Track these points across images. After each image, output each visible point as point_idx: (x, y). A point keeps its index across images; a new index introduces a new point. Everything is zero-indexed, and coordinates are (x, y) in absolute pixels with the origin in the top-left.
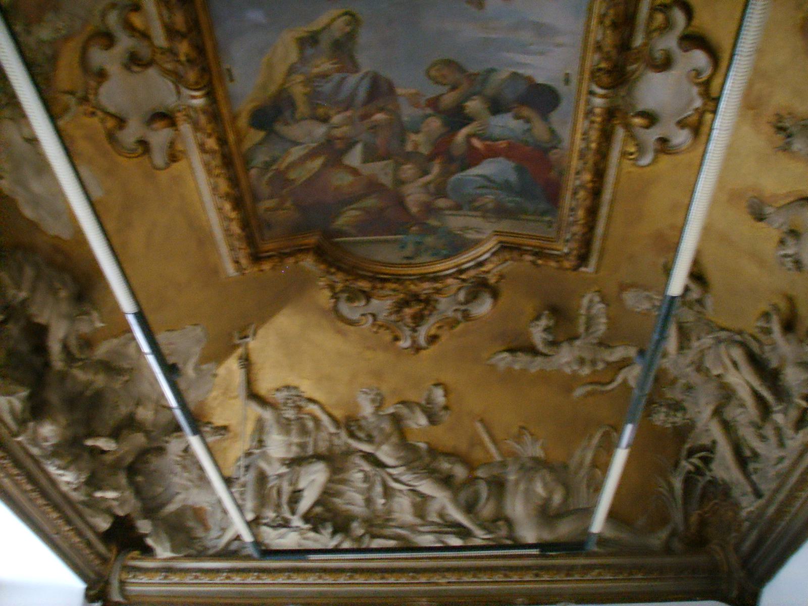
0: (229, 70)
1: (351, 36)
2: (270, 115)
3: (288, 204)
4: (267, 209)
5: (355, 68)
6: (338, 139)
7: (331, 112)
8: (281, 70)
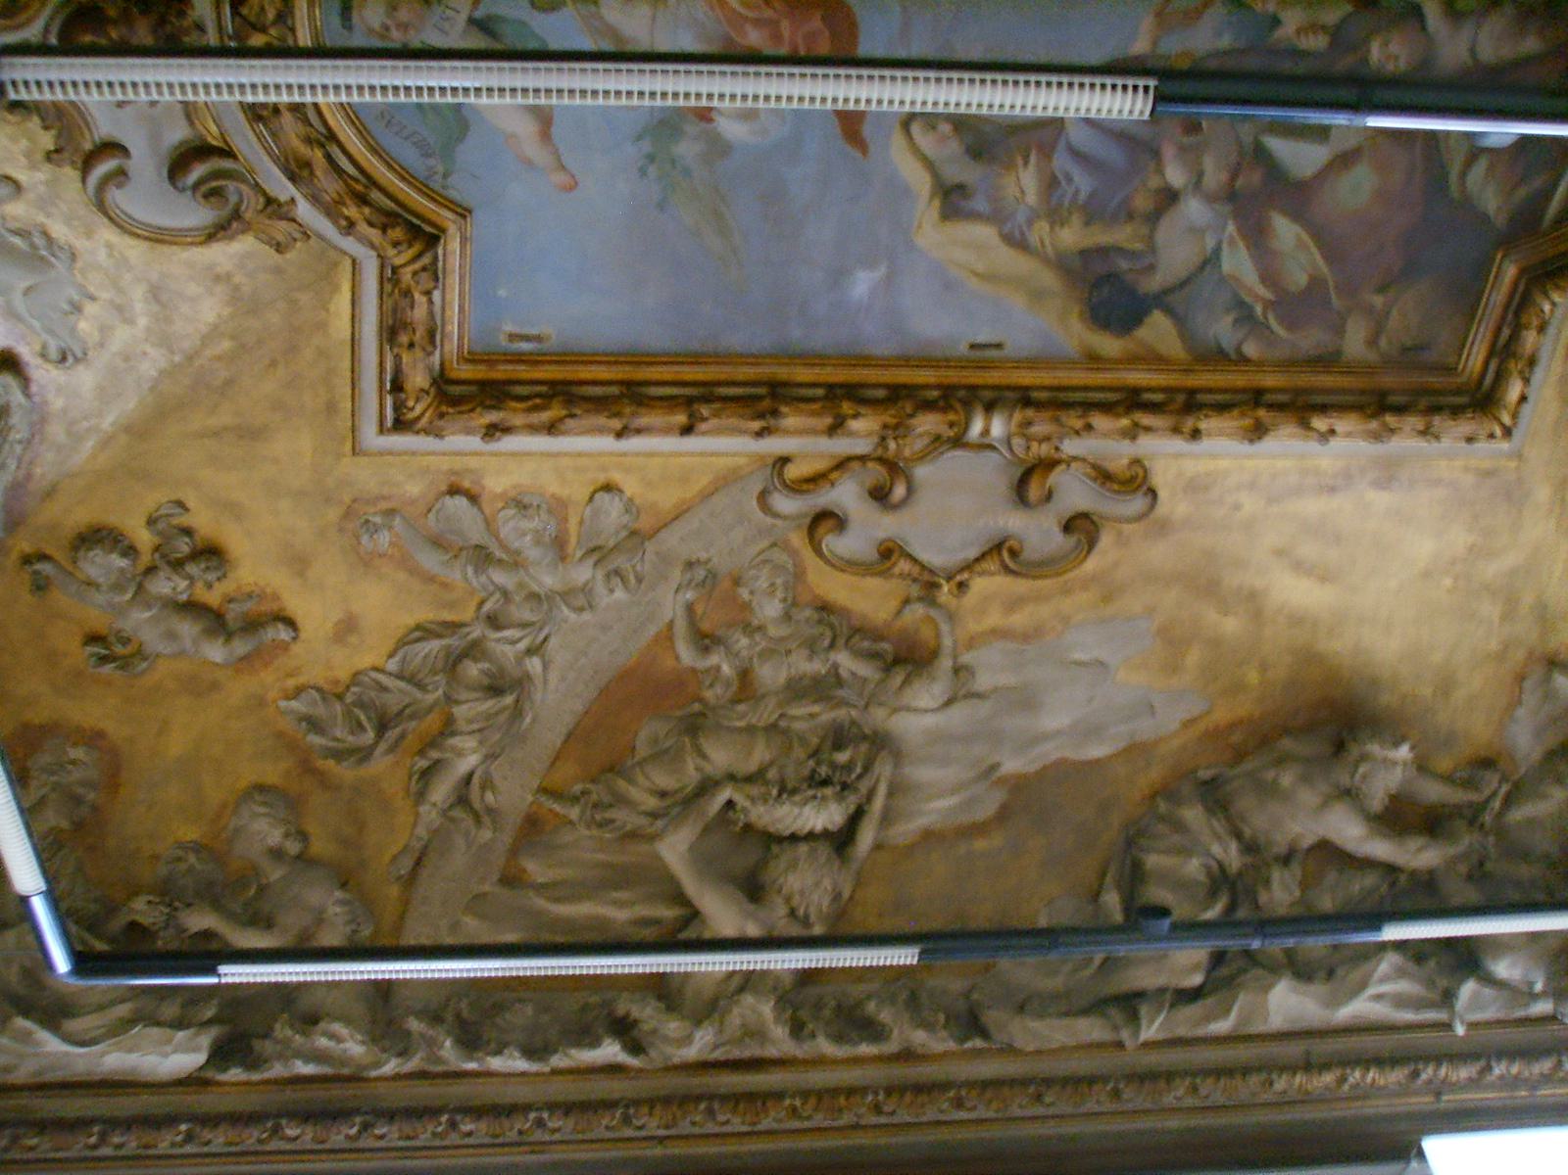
0: (973, 346)
2: (1111, 295)
3: (1378, 301)
4: (1372, 342)
6: (1234, 177)
7: (1154, 182)
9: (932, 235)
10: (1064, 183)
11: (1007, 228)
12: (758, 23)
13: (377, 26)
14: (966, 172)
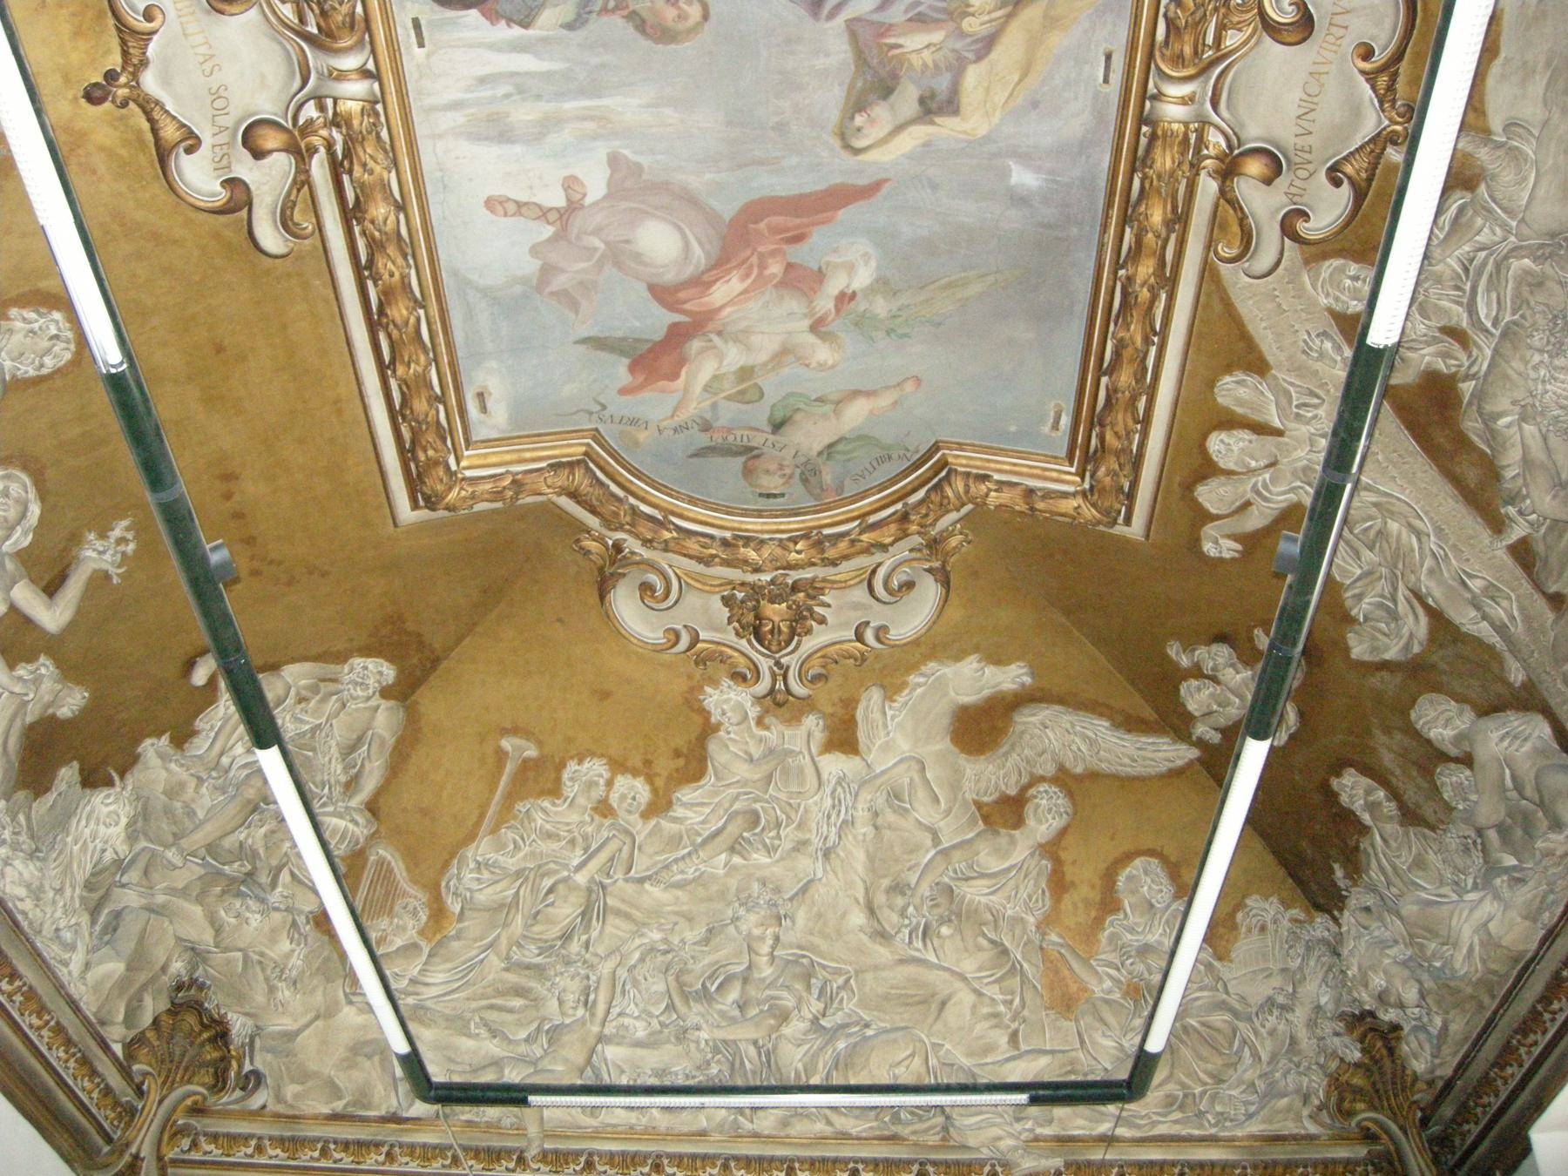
0: (1106, 80)
1: (858, 104)
5: (852, 27)
8: (1009, 50)
9: (972, 123)
10: (920, 9)
11: (971, 56)
12: (762, 266)
13: (781, 481)
14: (907, 99)
